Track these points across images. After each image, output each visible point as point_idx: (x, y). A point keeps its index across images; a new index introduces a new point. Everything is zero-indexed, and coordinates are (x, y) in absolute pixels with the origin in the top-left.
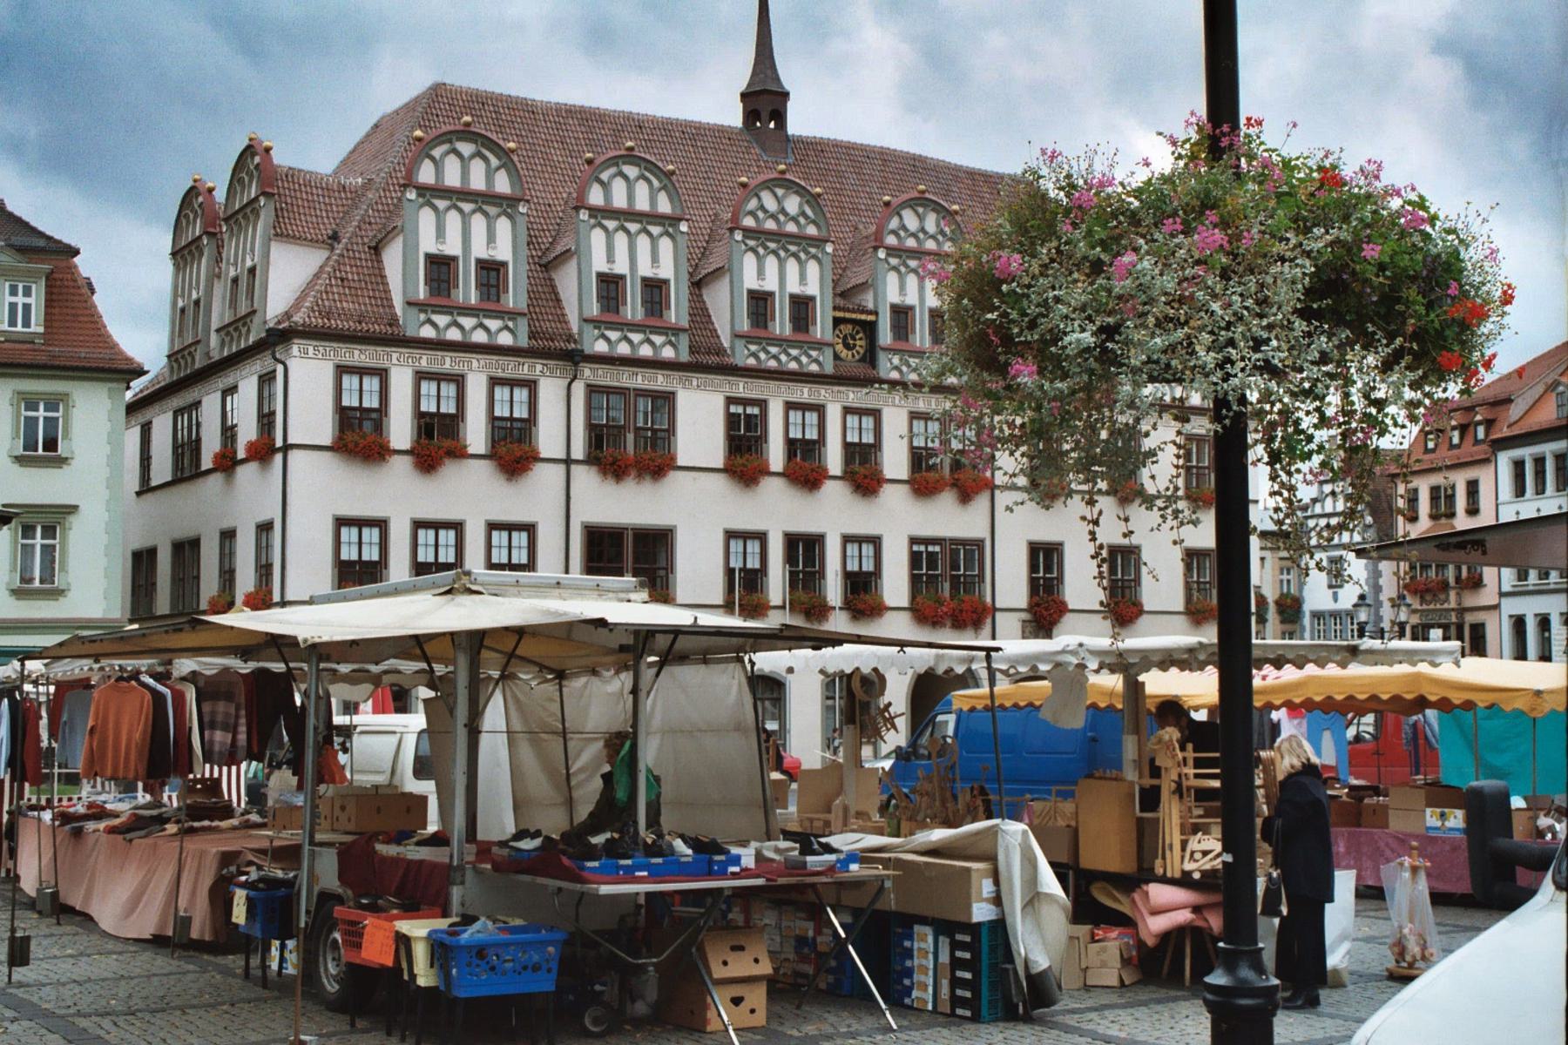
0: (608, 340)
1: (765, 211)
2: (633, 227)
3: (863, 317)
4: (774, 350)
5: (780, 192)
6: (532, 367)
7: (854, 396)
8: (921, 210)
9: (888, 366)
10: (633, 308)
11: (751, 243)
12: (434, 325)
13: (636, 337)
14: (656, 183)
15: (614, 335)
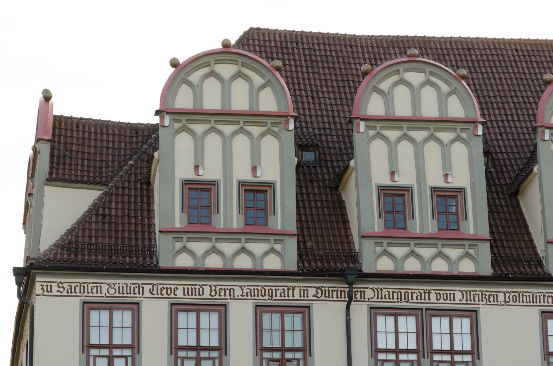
0: (391, 256)
2: (419, 135)
6: (304, 292)
10: (423, 220)
12: (191, 253)
13: (427, 252)
14: (445, 88)
15: (399, 251)
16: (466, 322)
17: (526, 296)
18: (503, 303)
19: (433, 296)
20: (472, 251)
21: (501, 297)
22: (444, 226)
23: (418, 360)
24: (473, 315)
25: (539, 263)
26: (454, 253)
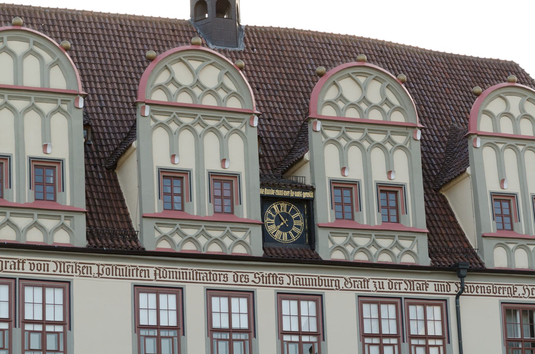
1: (178, 85)
3: (298, 194)
4: (191, 232)
5: (195, 65)
7: (289, 277)
8: (362, 80)
9: (328, 246)
11: (162, 119)
13: (22, 222)
14: (48, 58)
16: (59, 293)
17: (119, 269)
18: (97, 275)
19: (27, 266)
20: (68, 223)
21: (95, 269)
22: (41, 196)
23: (10, 330)
24: (66, 286)
25: (134, 237)
26: (49, 224)
